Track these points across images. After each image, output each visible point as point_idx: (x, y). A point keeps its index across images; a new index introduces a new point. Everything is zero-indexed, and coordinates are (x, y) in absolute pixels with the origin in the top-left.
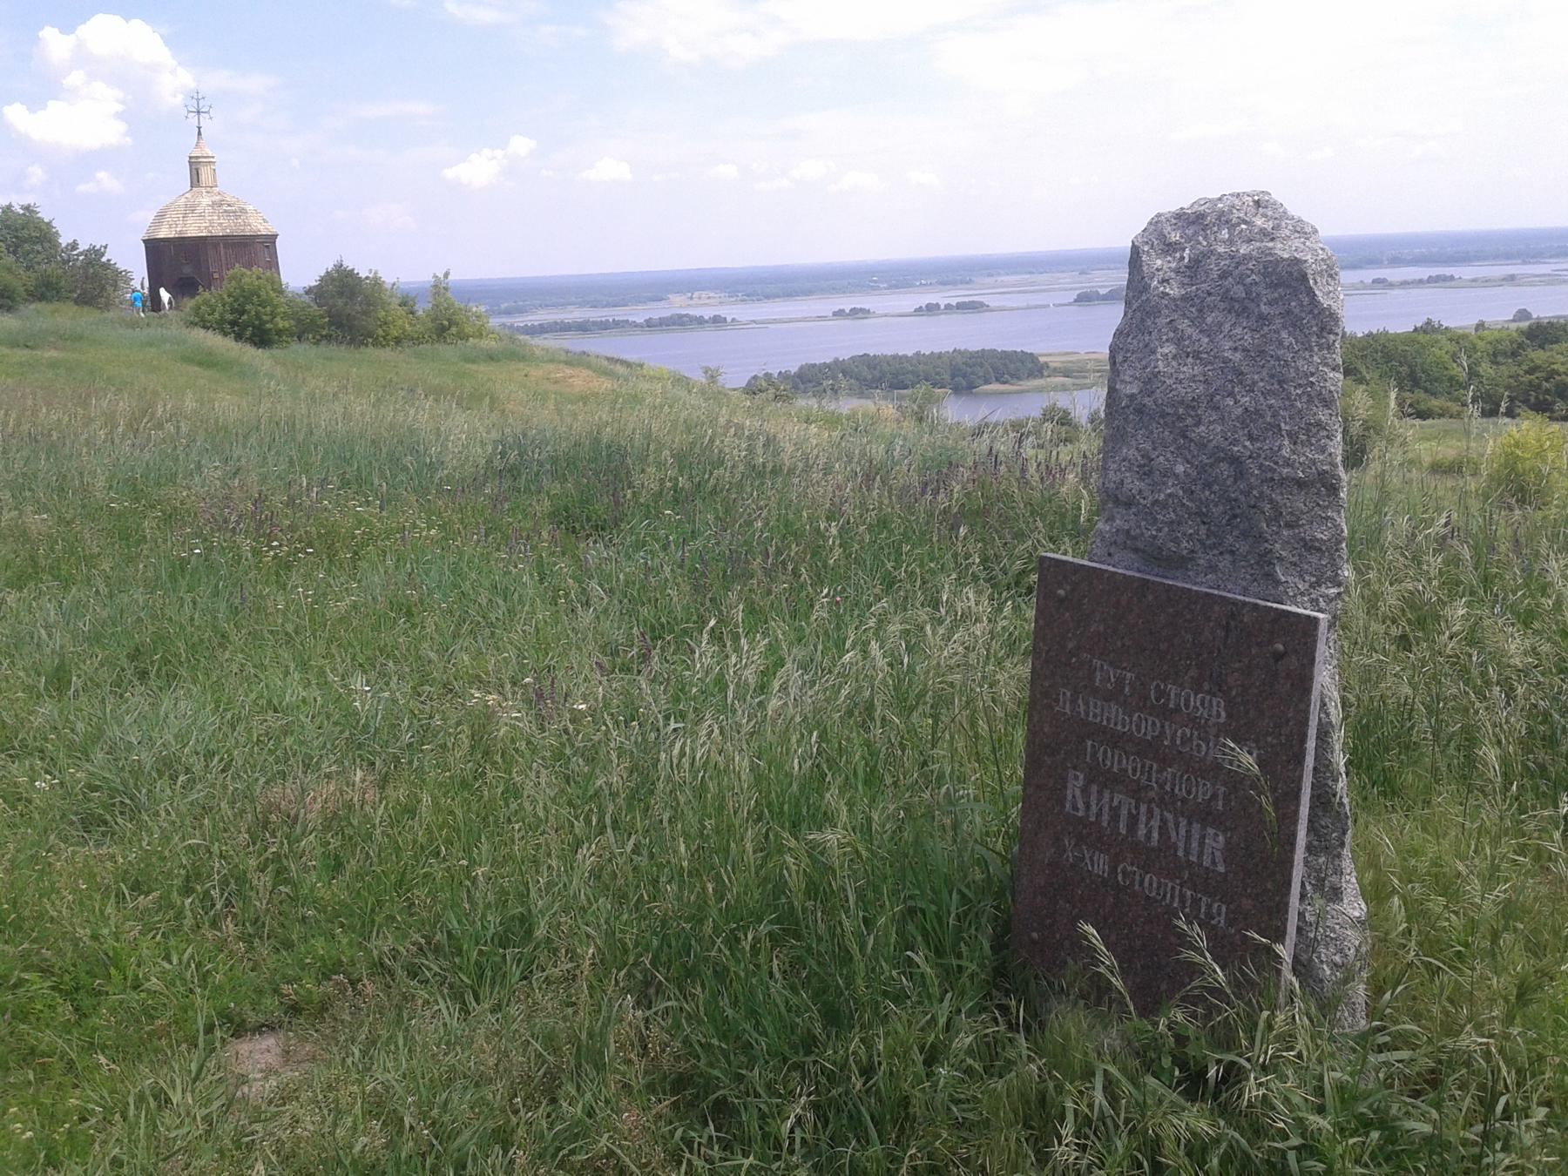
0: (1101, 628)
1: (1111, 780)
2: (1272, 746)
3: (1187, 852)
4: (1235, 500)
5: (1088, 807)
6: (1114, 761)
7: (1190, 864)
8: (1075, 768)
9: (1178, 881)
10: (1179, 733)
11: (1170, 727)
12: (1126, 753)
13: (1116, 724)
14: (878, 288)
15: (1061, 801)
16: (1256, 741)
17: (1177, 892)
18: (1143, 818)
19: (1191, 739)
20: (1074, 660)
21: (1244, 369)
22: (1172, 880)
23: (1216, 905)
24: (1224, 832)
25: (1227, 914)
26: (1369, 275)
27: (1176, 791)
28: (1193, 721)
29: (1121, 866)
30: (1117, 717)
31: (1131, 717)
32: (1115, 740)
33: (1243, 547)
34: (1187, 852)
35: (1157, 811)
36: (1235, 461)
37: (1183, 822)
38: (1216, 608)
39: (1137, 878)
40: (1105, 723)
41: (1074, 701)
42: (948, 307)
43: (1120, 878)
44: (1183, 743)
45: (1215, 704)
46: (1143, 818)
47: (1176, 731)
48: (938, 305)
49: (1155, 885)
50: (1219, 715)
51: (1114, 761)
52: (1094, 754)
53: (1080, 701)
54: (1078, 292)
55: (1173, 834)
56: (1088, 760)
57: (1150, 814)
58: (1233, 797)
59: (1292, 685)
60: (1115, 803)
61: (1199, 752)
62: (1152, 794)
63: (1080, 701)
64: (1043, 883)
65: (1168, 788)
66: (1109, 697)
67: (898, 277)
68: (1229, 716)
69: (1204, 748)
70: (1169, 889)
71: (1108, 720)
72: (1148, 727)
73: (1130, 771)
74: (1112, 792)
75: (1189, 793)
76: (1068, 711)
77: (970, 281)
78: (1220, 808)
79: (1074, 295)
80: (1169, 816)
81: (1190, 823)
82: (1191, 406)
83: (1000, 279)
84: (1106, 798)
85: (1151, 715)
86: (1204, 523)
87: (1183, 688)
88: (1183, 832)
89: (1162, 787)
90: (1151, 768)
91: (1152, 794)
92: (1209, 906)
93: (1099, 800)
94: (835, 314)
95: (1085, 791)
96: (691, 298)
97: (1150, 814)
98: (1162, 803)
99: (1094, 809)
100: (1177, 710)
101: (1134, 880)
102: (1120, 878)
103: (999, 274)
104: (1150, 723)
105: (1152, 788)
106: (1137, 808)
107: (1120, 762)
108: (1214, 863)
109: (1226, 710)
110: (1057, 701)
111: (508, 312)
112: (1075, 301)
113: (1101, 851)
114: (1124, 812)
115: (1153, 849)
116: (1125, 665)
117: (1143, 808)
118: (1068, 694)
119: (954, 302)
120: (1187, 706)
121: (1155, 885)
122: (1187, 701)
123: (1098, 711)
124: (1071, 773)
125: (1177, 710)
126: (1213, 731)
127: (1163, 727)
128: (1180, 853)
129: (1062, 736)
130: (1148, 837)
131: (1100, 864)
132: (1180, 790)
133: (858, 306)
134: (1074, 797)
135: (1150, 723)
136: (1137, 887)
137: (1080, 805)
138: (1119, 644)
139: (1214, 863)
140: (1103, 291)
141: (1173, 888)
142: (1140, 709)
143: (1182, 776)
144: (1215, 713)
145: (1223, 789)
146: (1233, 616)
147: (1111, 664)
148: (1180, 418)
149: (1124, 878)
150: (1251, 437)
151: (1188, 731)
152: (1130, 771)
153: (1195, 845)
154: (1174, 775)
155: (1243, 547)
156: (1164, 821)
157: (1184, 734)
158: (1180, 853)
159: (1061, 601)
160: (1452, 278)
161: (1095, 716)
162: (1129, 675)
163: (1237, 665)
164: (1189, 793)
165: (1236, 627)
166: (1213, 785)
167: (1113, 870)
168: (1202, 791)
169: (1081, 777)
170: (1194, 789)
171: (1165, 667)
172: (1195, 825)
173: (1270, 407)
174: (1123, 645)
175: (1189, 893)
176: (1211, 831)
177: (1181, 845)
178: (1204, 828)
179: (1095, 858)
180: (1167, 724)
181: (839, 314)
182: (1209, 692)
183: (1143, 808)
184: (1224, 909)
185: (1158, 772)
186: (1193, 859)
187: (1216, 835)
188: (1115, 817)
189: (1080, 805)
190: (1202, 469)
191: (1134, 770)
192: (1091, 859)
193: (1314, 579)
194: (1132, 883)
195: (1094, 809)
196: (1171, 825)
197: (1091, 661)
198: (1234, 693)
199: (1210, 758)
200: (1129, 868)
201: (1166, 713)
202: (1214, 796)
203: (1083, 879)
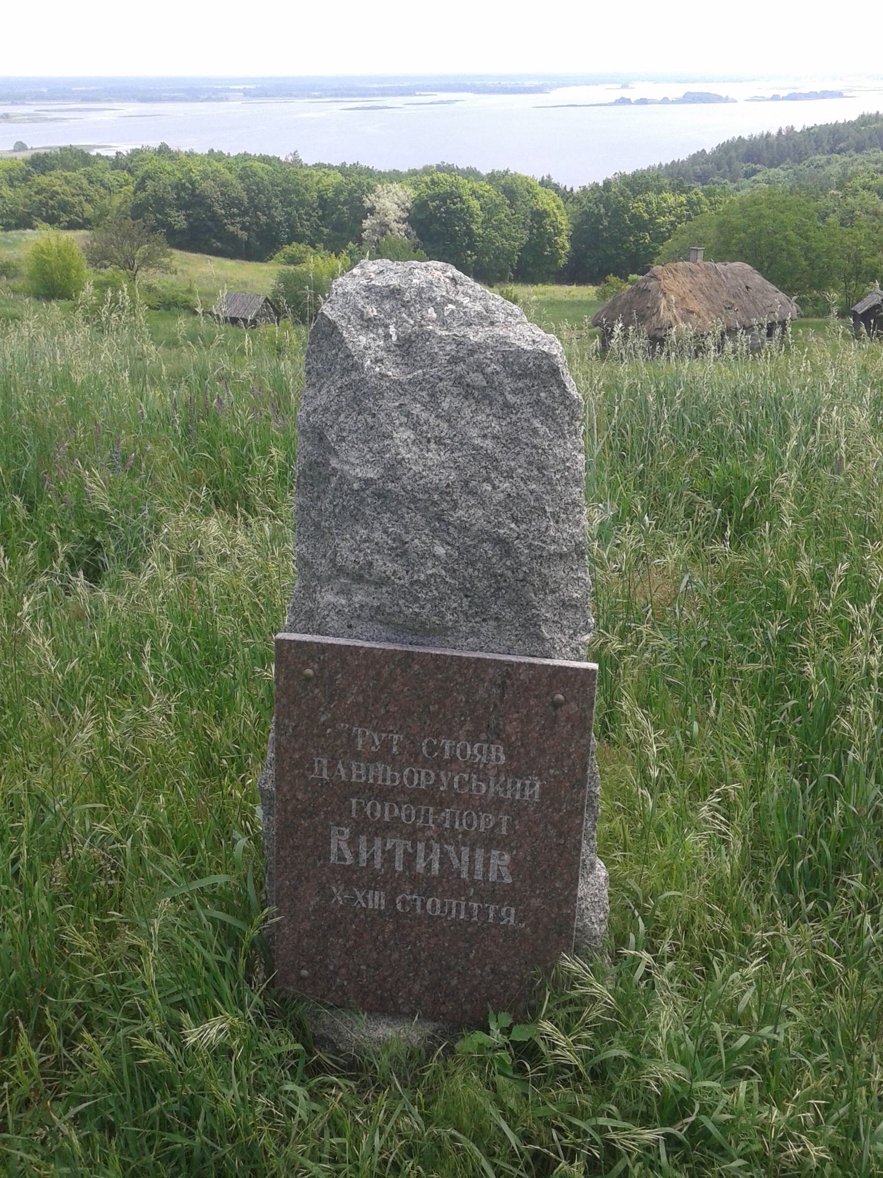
0: (360, 699)
1: (383, 829)
2: (555, 777)
3: (471, 873)
4: (501, 575)
5: (356, 855)
6: (383, 812)
7: (474, 883)
8: (338, 825)
9: (463, 898)
10: (456, 779)
11: (446, 775)
12: (397, 803)
13: (384, 780)
15: (326, 856)
16: (539, 775)
17: (463, 907)
18: (421, 854)
19: (470, 781)
20: (329, 731)
21: (499, 456)
22: (456, 898)
23: (504, 909)
24: (510, 851)
25: (516, 914)
27: (457, 826)
28: (472, 767)
29: (400, 897)
30: (384, 774)
31: (401, 772)
32: (383, 794)
33: (508, 614)
34: (471, 873)
35: (436, 846)
36: (499, 541)
37: (465, 851)
38: (490, 671)
39: (419, 903)
40: (371, 781)
41: (332, 767)
43: (399, 906)
44: (461, 786)
45: (493, 749)
46: (421, 854)
47: (453, 778)
49: (438, 906)
50: (498, 758)
51: (383, 812)
52: (361, 810)
53: (340, 766)
55: (455, 862)
56: (354, 815)
57: (429, 849)
58: (517, 822)
59: (573, 726)
60: (389, 846)
61: (479, 791)
62: (429, 833)
63: (340, 766)
64: (308, 928)
65: (447, 825)
66: (373, 759)
68: (509, 757)
69: (484, 787)
70: (454, 905)
71: (375, 778)
72: (422, 779)
73: (403, 818)
74: (383, 838)
75: (470, 826)
76: (325, 776)
78: (504, 833)
80: (450, 848)
81: (473, 850)
82: (446, 491)
84: (378, 842)
85: (424, 768)
86: (467, 596)
87: (457, 740)
88: (465, 858)
89: (439, 826)
90: (427, 811)
91: (429, 833)
92: (497, 912)
93: (369, 848)
95: (353, 842)
97: (429, 849)
98: (441, 838)
99: (364, 856)
100: (453, 759)
101: (415, 906)
102: (399, 906)
104: (423, 774)
105: (430, 828)
106: (414, 847)
107: (391, 811)
108: (500, 876)
109: (505, 753)
110: (312, 769)
113: (375, 889)
114: (399, 854)
115: (434, 877)
116: (391, 728)
117: (421, 846)
118: (325, 762)
120: (463, 755)
121: (438, 906)
122: (463, 753)
123: (362, 772)
124: (334, 830)
125: (453, 759)
126: (492, 773)
127: (437, 775)
128: (464, 875)
129: (321, 800)
130: (428, 868)
131: (377, 900)
132: (461, 824)
134: (339, 849)
135: (423, 774)
136: (419, 911)
137: (348, 855)
138: (383, 711)
139: (500, 876)
141: (458, 905)
142: (410, 764)
143: (461, 814)
144: (493, 757)
145: (506, 818)
146: (508, 675)
147: (375, 730)
148: (435, 503)
149: (403, 907)
150: (515, 519)
151: (466, 776)
152: (403, 818)
153: (479, 866)
154: (453, 815)
155: (508, 614)
156: (444, 854)
157: (461, 778)
158: (464, 875)
159: (308, 679)
161: (359, 776)
162: (396, 736)
163: (516, 716)
164: (470, 826)
165: (513, 685)
166: (496, 816)
167: (391, 902)
168: (483, 823)
169: (347, 831)
170: (475, 823)
171: (437, 726)
172: (478, 850)
173: (532, 492)
174: (388, 712)
175: (475, 905)
176: (495, 853)
177: (465, 869)
178: (487, 851)
179: (369, 896)
180: (442, 773)
182: (486, 741)
183: (421, 846)
184: (513, 911)
185: (435, 814)
186: (479, 877)
187: (501, 855)
188: (389, 857)
189: (348, 855)
190: (464, 550)
191: (409, 817)
192: (365, 898)
193: (571, 632)
194: (414, 909)
195: (364, 856)
196: (453, 855)
197: (350, 730)
198: (513, 739)
199: (491, 794)
200: (409, 898)
201: (440, 764)
202: (498, 824)
203: (356, 916)
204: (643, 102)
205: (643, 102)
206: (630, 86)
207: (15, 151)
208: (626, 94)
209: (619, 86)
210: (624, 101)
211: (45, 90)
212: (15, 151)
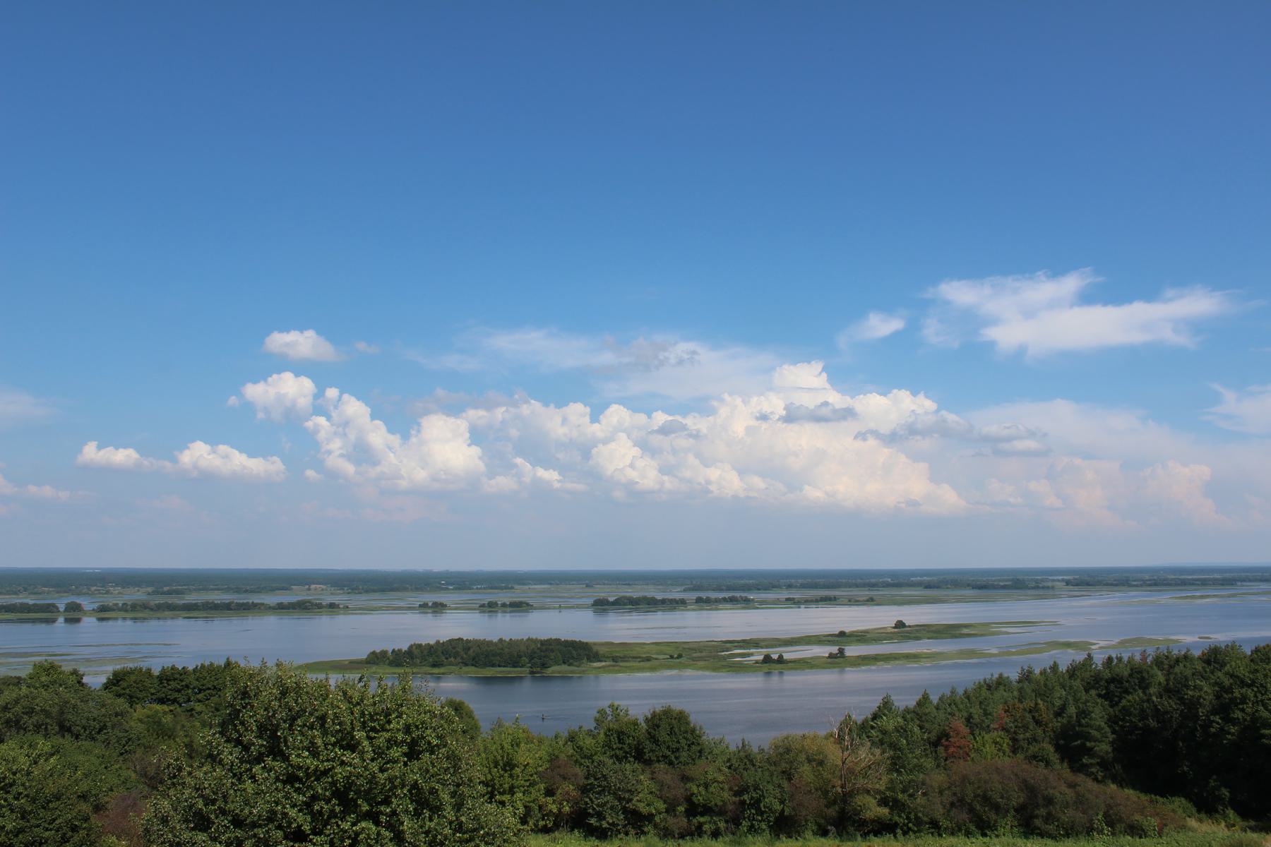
14: (447, 589)
26: (784, 594)
42: (504, 605)
48: (496, 604)
54: (595, 599)
67: (462, 582)
77: (512, 588)
79: (591, 601)
83: (531, 587)
94: (421, 606)
96: (309, 589)
103: (529, 584)
111: (170, 593)
112: (593, 605)
119: (507, 601)
133: (439, 600)
140: (611, 599)
181: (424, 606)
207: (894, 628)
211: (889, 580)
212: (894, 628)
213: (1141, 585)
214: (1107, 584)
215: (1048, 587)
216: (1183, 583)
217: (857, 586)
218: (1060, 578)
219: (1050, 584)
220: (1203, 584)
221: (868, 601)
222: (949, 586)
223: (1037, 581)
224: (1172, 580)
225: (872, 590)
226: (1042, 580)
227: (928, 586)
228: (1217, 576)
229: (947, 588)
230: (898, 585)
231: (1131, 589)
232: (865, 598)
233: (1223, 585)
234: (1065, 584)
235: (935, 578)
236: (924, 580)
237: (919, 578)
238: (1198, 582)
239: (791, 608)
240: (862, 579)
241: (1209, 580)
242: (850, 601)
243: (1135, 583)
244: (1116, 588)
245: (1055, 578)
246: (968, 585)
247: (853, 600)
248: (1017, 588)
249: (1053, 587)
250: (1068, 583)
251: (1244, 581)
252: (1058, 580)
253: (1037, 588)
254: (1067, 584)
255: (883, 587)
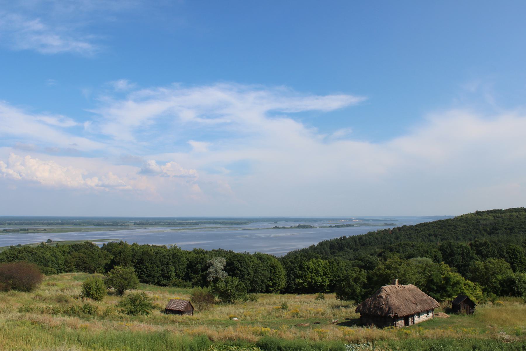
160: (28, 230)
204: (283, 228)
205: (283, 228)
206: (278, 222)
208: (277, 225)
209: (274, 222)
210: (277, 228)
212: (46, 242)
213: (163, 225)
214: (151, 224)
215: (126, 225)
216: (180, 224)
217: (43, 224)
218: (134, 221)
219: (126, 224)
220: (187, 224)
221: (43, 231)
222: (84, 224)
223: (124, 223)
224: (177, 222)
225: (49, 226)
226: (126, 222)
227: (75, 224)
228: (195, 221)
229: (84, 225)
230: (62, 224)
231: (159, 226)
232: (42, 230)
233: (193, 225)
234: (134, 224)
235: (81, 221)
236: (76, 222)
237: (75, 221)
238: (185, 224)
239: (4, 234)
240: (48, 221)
241: (189, 223)
242: (34, 231)
243: (161, 224)
244: (154, 226)
245: (132, 221)
246: (93, 224)
247: (36, 230)
248: (113, 225)
249: (128, 225)
250: (135, 223)
251: (202, 223)
252: (133, 222)
253: (122, 225)
254: (135, 224)
255: (55, 224)
